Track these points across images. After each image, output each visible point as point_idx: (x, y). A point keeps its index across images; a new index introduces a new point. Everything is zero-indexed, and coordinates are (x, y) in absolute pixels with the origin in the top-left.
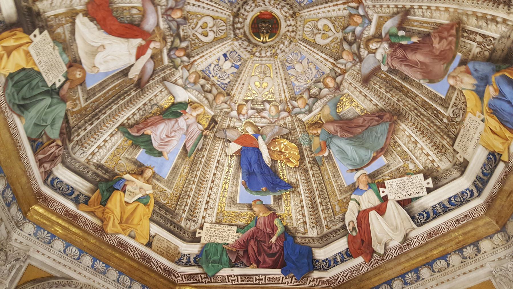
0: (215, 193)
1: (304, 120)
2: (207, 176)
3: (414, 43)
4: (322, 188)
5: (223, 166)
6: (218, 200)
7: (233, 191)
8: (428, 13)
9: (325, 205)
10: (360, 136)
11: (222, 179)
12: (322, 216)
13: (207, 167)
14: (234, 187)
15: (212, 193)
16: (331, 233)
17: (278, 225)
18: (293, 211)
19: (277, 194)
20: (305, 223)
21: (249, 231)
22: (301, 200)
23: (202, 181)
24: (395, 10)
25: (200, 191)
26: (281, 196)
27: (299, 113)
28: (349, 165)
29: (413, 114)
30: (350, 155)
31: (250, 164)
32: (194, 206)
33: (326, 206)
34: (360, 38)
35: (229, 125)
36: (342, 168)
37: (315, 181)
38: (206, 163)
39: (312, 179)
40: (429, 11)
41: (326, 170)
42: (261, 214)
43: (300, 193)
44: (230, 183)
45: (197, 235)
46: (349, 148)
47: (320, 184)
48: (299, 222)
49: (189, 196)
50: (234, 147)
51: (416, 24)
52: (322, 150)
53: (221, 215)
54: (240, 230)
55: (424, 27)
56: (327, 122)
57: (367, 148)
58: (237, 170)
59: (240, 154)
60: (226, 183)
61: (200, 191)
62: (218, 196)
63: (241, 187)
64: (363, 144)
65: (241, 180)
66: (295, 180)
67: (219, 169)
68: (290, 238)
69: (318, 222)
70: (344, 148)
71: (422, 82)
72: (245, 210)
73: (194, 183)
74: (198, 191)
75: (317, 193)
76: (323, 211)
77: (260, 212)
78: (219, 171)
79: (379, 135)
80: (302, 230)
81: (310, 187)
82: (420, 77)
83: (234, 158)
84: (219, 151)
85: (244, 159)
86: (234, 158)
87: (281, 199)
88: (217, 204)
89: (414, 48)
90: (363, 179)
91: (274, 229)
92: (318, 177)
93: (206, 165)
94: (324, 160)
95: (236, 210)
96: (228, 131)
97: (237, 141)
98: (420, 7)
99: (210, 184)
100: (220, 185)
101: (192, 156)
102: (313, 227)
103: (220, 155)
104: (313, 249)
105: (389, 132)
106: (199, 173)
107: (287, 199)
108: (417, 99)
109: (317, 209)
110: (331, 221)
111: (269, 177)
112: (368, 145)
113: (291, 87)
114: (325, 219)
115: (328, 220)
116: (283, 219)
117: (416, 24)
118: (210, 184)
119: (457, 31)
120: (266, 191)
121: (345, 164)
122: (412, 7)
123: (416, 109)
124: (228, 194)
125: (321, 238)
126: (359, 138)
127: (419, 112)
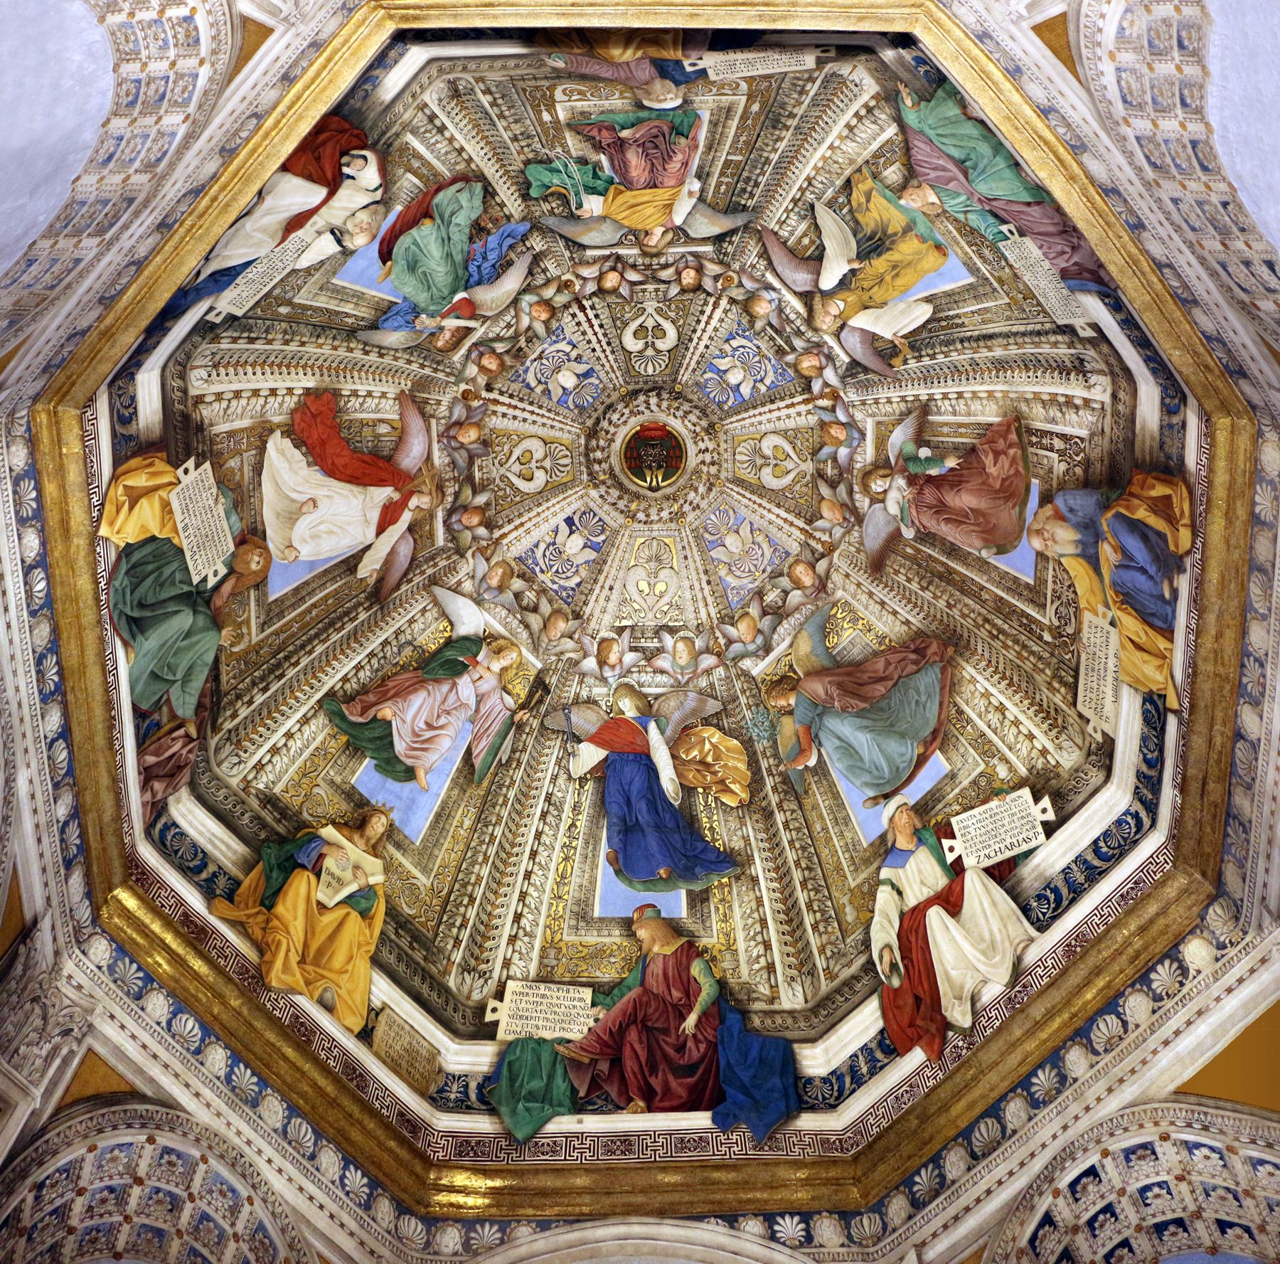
0: (537, 889)
1: (754, 672)
2: (519, 840)
3: (952, 470)
4: (809, 859)
5: (560, 810)
6: (544, 910)
7: (585, 883)
8: (961, 407)
9: (820, 910)
10: (883, 704)
11: (558, 847)
12: (814, 941)
13: (519, 813)
14: (587, 868)
15: (531, 890)
16: (838, 991)
17: (702, 979)
18: (740, 935)
19: (697, 887)
20: (771, 968)
21: (625, 999)
22: (759, 902)
23: (506, 855)
24: (903, 405)
25: (499, 883)
26: (707, 891)
27: (743, 656)
28: (866, 784)
29: (983, 633)
30: (867, 759)
31: (628, 802)
32: (482, 928)
33: (823, 912)
34: (850, 469)
35: (577, 695)
36: (853, 793)
37: (791, 842)
38: (519, 802)
39: (785, 837)
40: (962, 402)
41: (815, 807)
42: (656, 949)
43: (755, 880)
44: (577, 858)
45: (489, 1017)
46: (862, 740)
47: (804, 848)
48: (756, 966)
49: (472, 900)
50: (590, 756)
51: (945, 430)
52: (802, 752)
53: (552, 953)
54: (601, 997)
55: (961, 435)
56: (808, 674)
57: (903, 735)
58: (594, 822)
59: (601, 773)
60: (566, 859)
61: (499, 883)
62: (546, 898)
63: (604, 869)
64: (892, 725)
65: (604, 848)
66: (742, 844)
67: (549, 819)
68: (733, 1018)
69: (804, 966)
70: (852, 740)
71: (984, 554)
72: (614, 938)
73: (486, 859)
74: (496, 883)
75: (797, 876)
76: (815, 927)
77: (654, 941)
78: (550, 825)
79: (924, 698)
80: (764, 990)
81: (780, 861)
82: (978, 543)
83: (589, 786)
84: (551, 767)
85: (613, 788)
86: (589, 786)
87: (707, 899)
88: (542, 922)
89: (952, 480)
90: (904, 819)
91: (690, 989)
92: (798, 830)
93: (518, 807)
94: (810, 779)
95: (592, 939)
96: (574, 710)
97: (596, 739)
98: (945, 396)
99: (525, 864)
100: (553, 866)
101: (485, 783)
102: (793, 979)
103: (554, 778)
104: (796, 1046)
105: (942, 688)
106: (498, 831)
107: (723, 900)
108: (985, 596)
109: (801, 923)
110: (837, 955)
111: (676, 837)
112: (903, 726)
113: (722, 595)
114: (822, 950)
115: (829, 954)
116: (714, 959)
117: (945, 430)
118: (525, 864)
119: (1019, 435)
120: (669, 878)
121: (858, 783)
122: (931, 398)
123: (987, 620)
124: (571, 891)
125: (815, 1011)
126: (882, 710)
127: (994, 626)
